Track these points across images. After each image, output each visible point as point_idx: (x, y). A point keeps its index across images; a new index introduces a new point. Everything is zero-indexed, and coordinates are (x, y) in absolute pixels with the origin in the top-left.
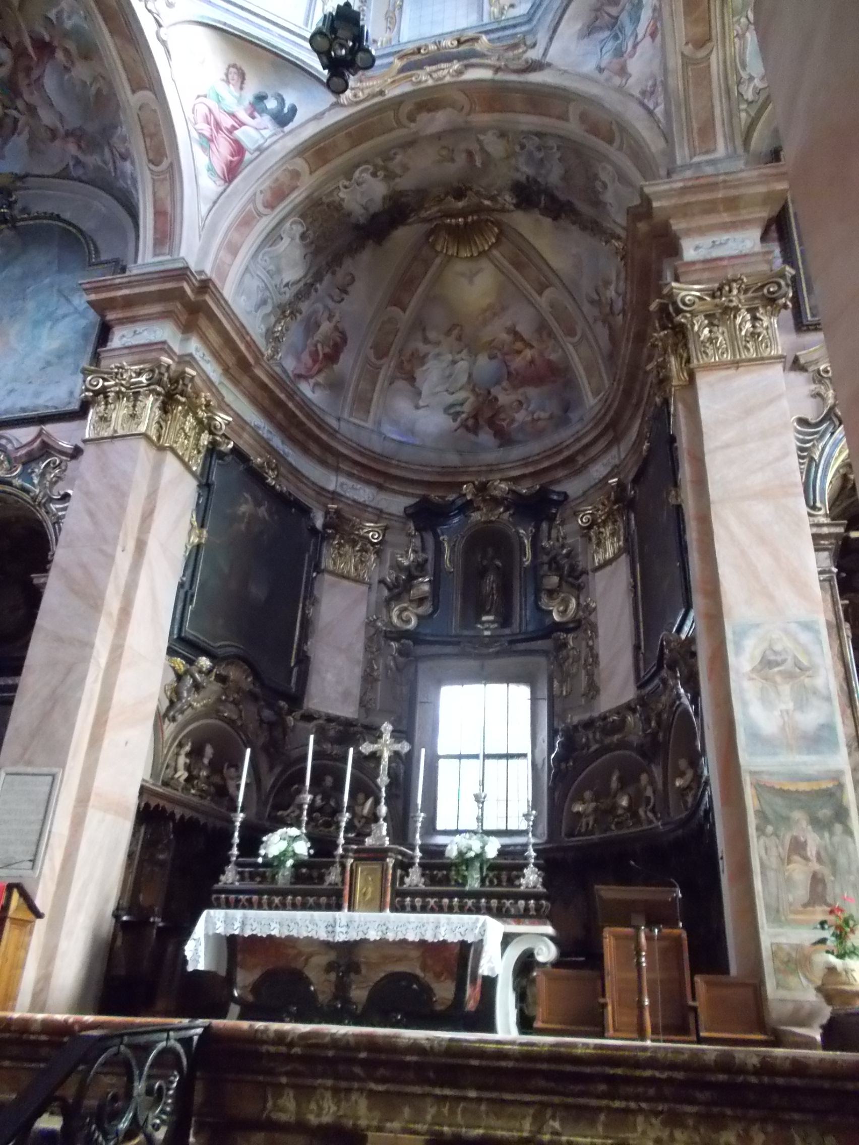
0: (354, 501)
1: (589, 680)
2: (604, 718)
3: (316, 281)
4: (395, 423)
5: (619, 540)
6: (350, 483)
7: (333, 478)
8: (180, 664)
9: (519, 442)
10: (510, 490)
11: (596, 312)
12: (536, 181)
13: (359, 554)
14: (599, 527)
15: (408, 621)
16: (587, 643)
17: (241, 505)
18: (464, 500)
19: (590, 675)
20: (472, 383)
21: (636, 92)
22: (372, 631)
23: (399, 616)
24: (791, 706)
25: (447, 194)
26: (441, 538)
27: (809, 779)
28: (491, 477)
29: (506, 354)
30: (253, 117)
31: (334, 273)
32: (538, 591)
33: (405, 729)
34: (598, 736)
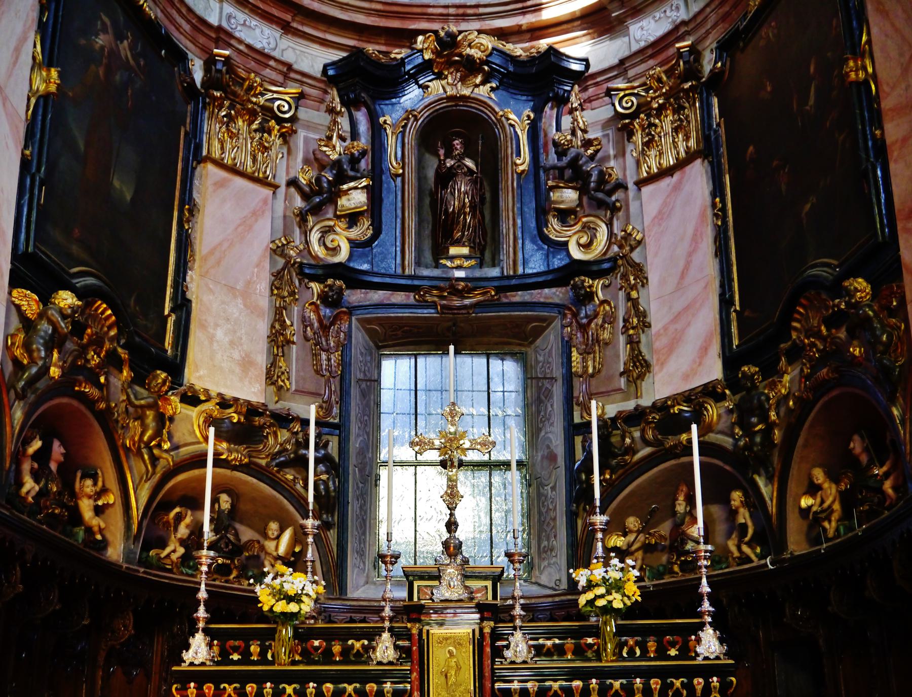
0: (249, 46)
1: (632, 349)
2: (661, 407)
5: (687, 138)
6: (241, 16)
8: (29, 302)
10: (493, 49)
13: (258, 136)
14: (649, 116)
15: (335, 250)
16: (628, 295)
17: (97, 36)
18: (420, 60)
19: (633, 343)
22: (281, 262)
23: (322, 242)
26: (381, 120)
28: (464, 26)
32: (543, 210)
33: (337, 421)
34: (650, 435)
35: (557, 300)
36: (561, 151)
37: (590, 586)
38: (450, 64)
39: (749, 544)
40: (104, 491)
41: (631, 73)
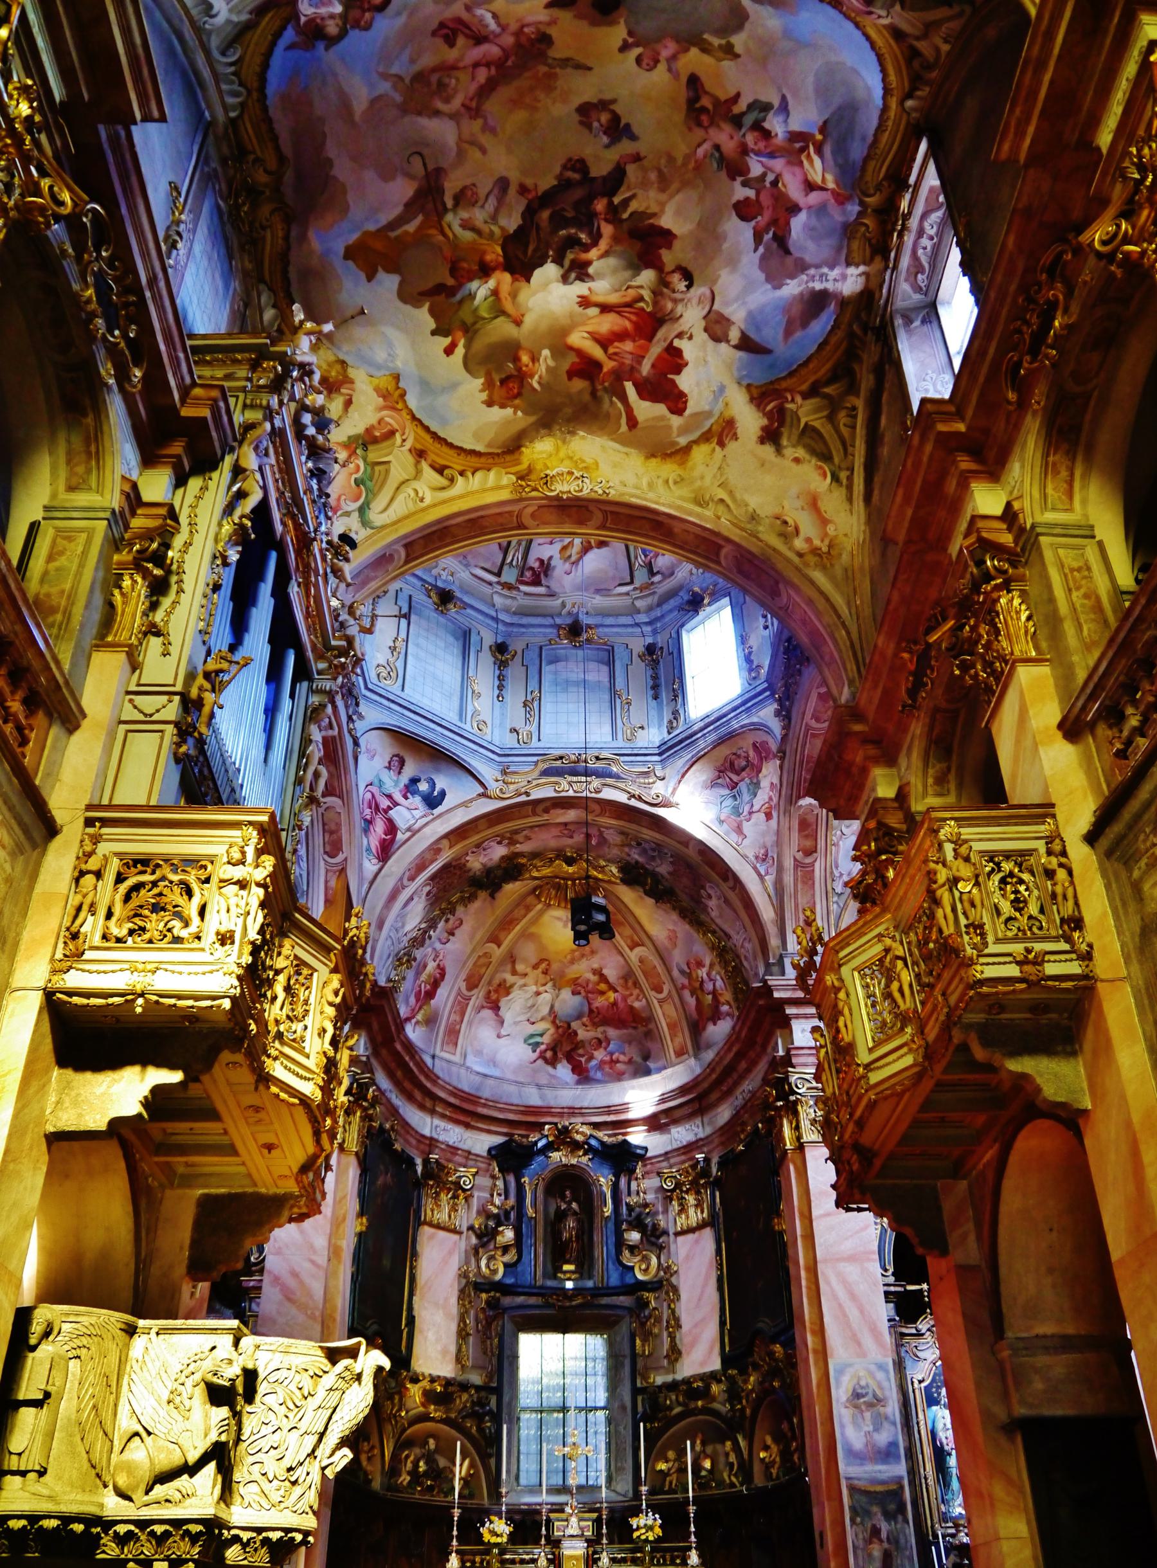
2: (687, 1381)
3: (430, 927)
4: (479, 1053)
6: (442, 1124)
7: (428, 1119)
9: (598, 1081)
11: (686, 982)
12: (646, 869)
15: (495, 1272)
19: (672, 1337)
20: (553, 1016)
21: (751, 856)
22: (464, 1281)
23: (488, 1266)
24: (871, 1428)
25: (558, 857)
27: (883, 1483)
28: (573, 1120)
29: (588, 992)
30: (406, 798)
31: (447, 921)
35: (627, 1304)
36: (630, 1208)
37: (638, 1528)
38: (564, 1143)
39: (736, 1475)
40: (372, 1448)
41: (672, 1161)
